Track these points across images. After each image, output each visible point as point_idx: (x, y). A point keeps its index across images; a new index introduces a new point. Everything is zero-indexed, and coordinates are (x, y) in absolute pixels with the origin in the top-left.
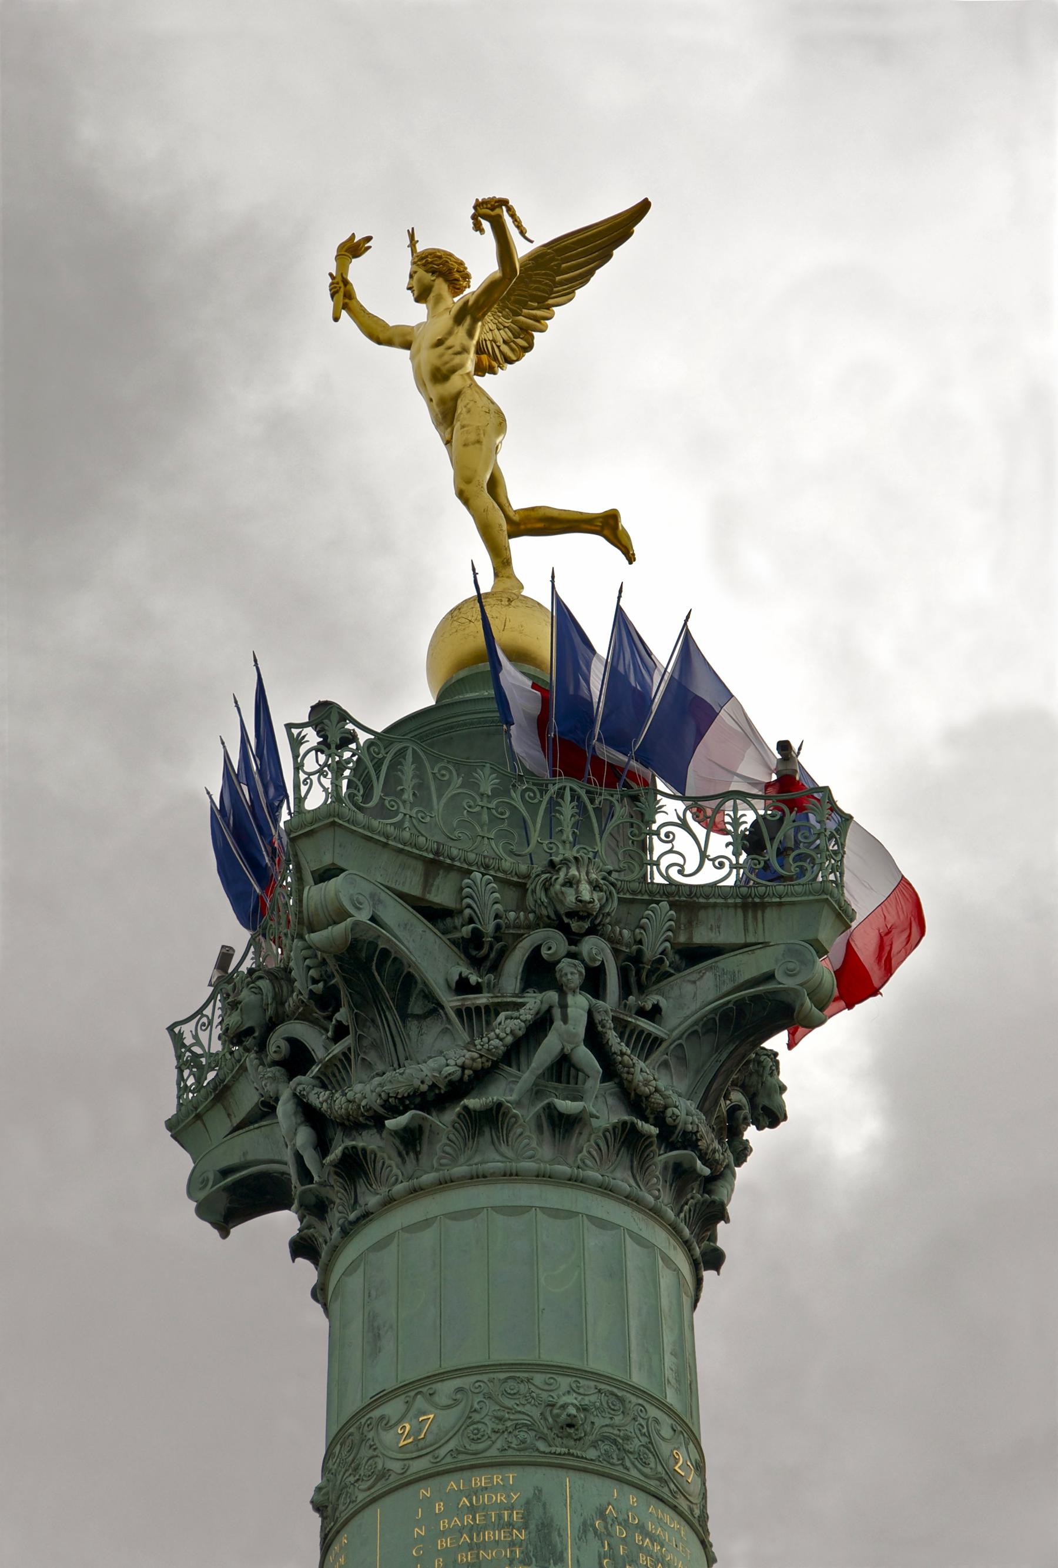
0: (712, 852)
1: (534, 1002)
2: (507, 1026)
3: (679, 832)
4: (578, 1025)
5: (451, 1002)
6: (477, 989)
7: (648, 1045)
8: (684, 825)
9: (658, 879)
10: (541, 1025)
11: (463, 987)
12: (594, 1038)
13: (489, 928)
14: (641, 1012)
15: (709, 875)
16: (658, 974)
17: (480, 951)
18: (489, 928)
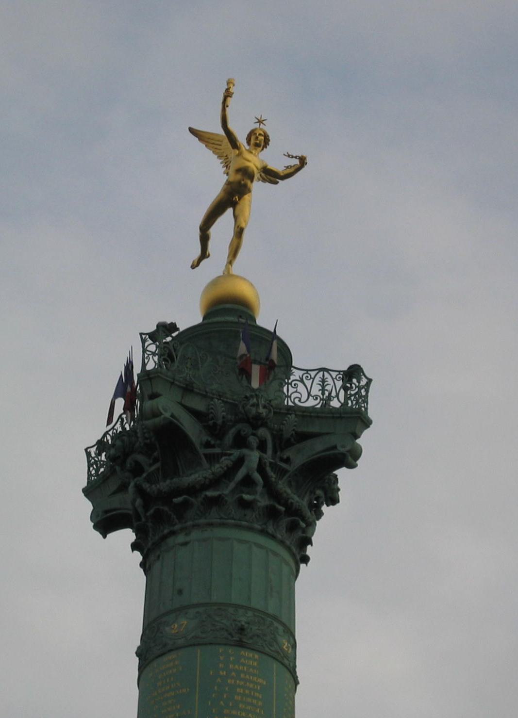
0: (313, 393)
1: (236, 453)
2: (226, 462)
3: (300, 384)
4: (255, 465)
5: (202, 451)
6: (213, 446)
7: (282, 472)
8: (302, 381)
9: (290, 404)
10: (240, 462)
11: (208, 445)
12: (261, 469)
13: (220, 422)
14: (282, 460)
15: (311, 403)
16: (288, 444)
17: (216, 431)
18: (220, 422)
